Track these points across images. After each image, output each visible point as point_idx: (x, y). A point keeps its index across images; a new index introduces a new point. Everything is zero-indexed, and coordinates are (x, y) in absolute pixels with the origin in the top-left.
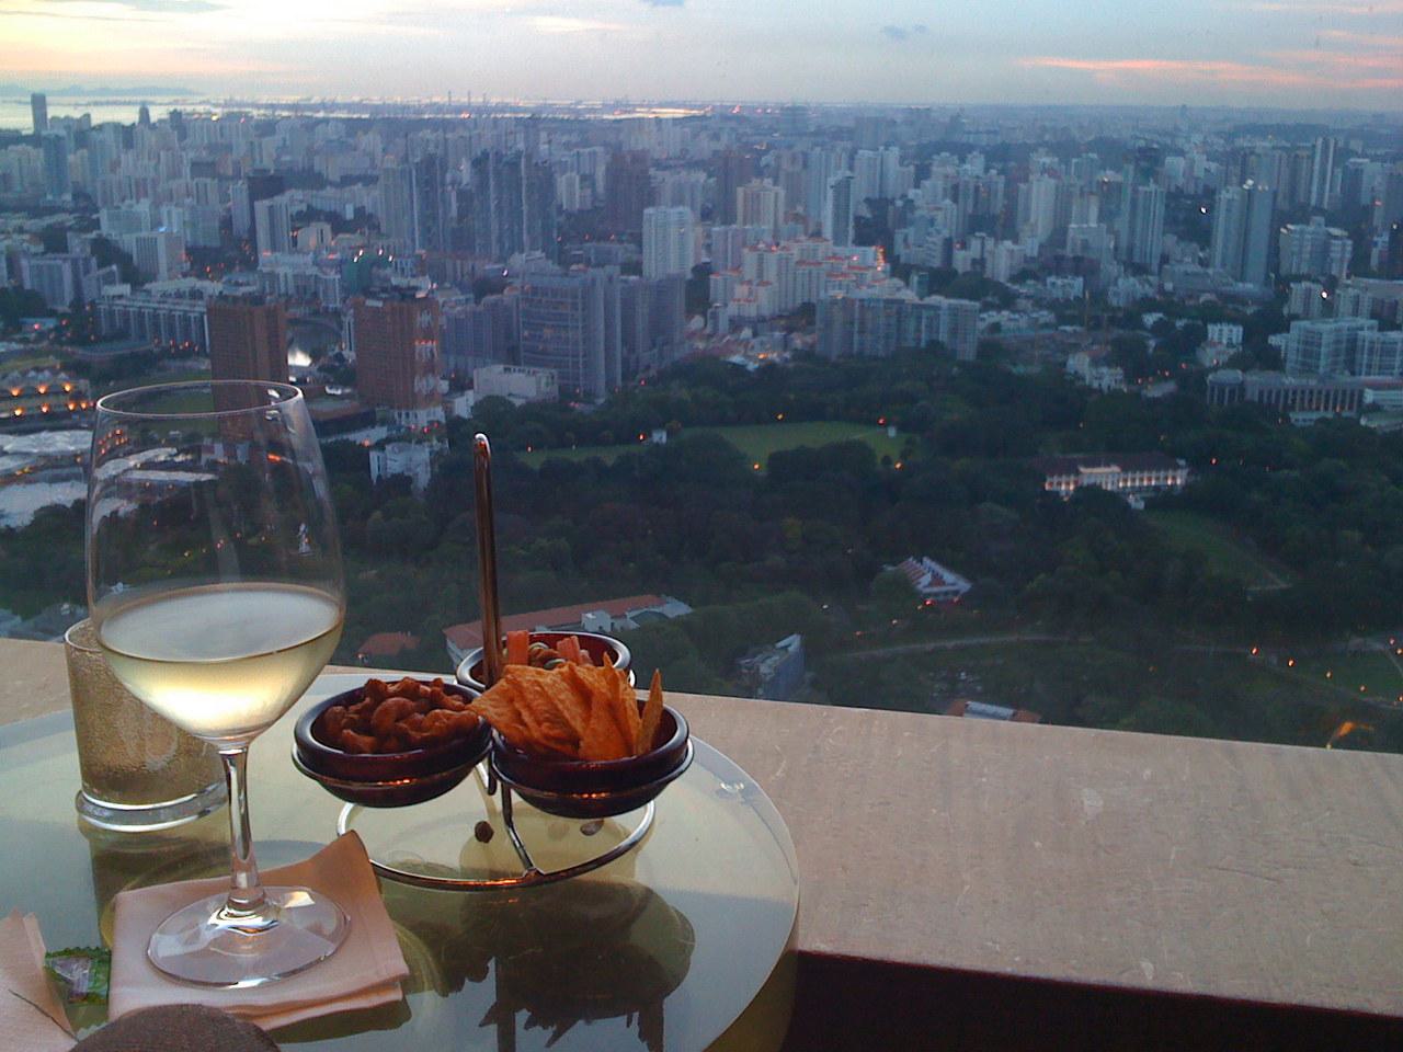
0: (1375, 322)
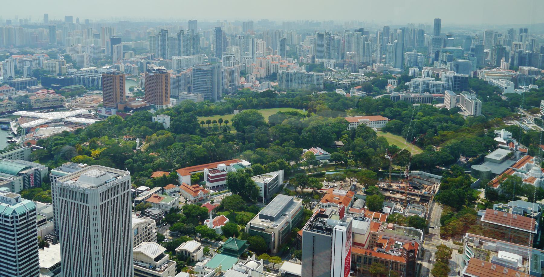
0: (434, 79)
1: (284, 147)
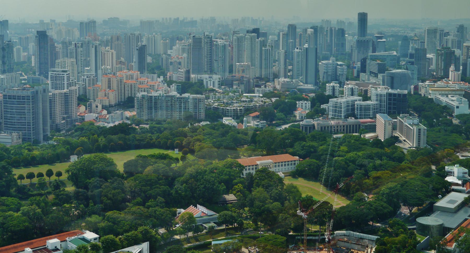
0: (361, 98)
1: (148, 207)
